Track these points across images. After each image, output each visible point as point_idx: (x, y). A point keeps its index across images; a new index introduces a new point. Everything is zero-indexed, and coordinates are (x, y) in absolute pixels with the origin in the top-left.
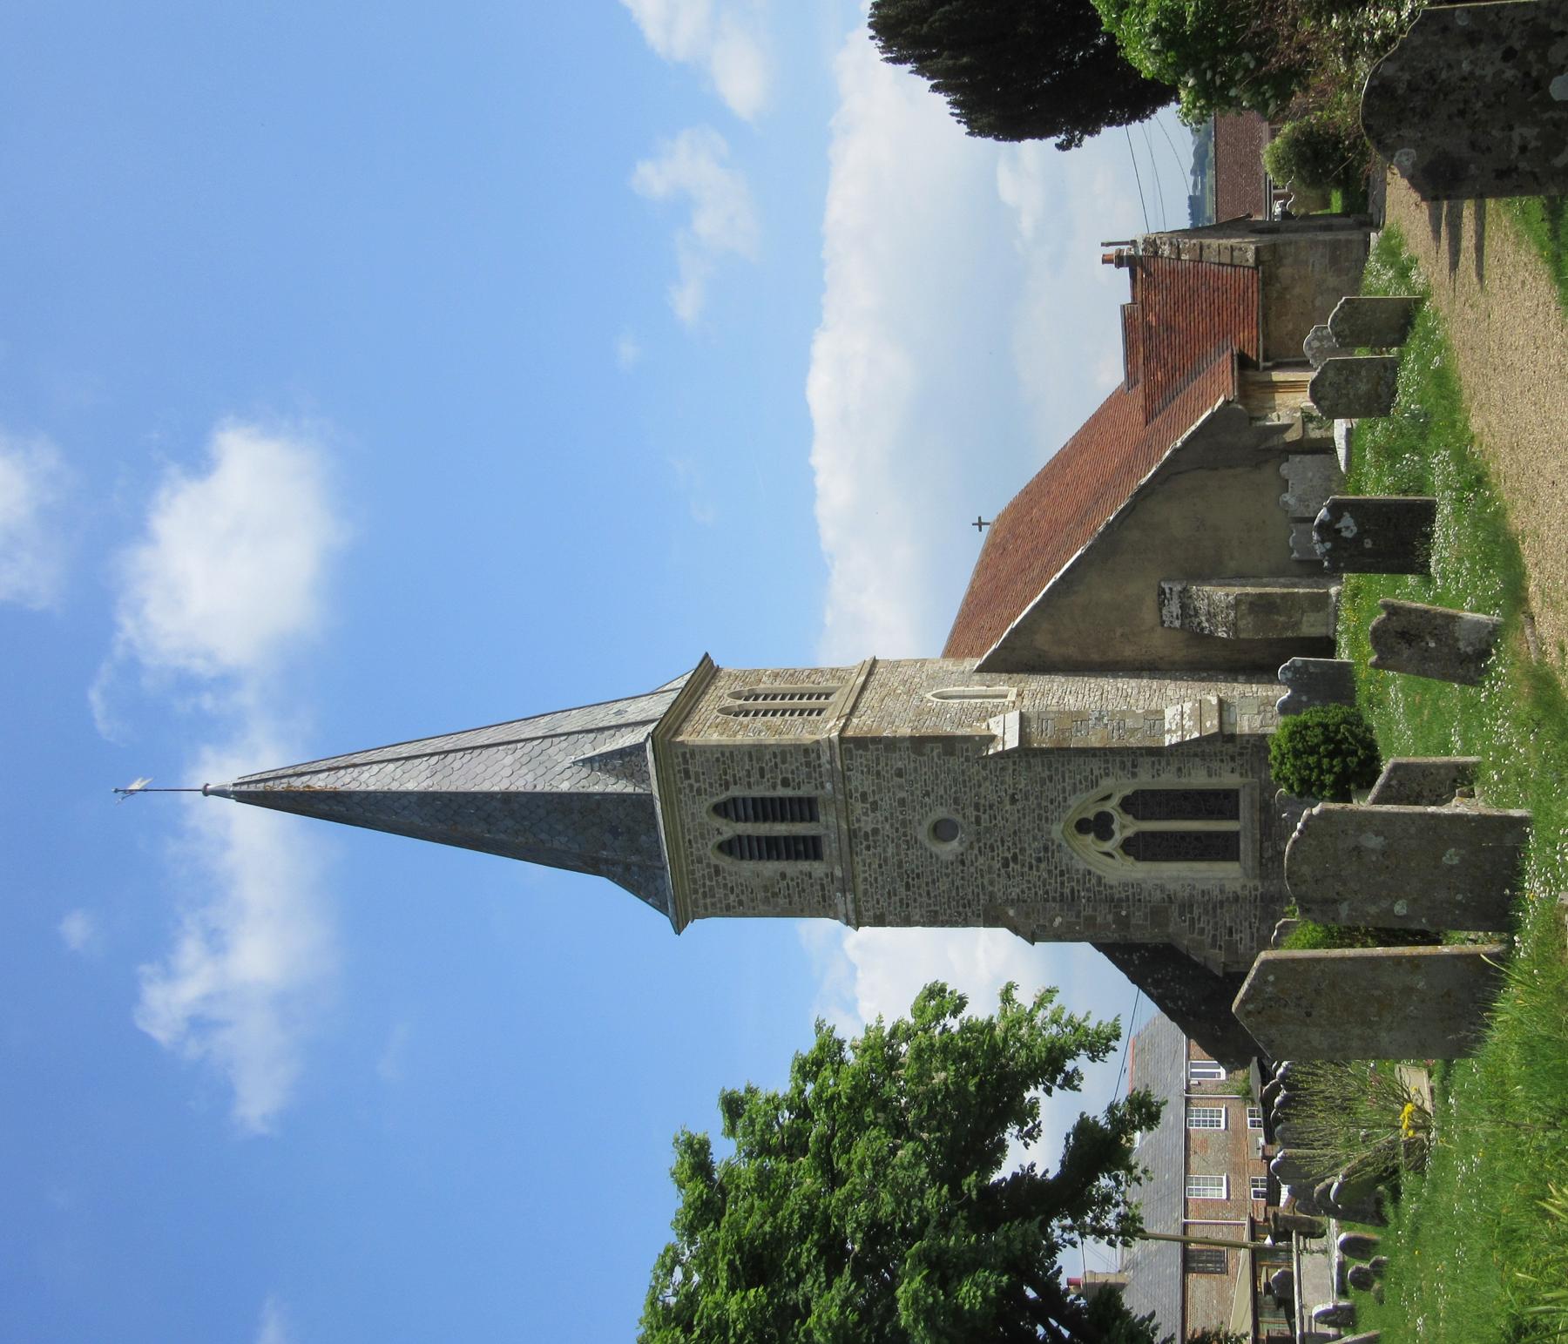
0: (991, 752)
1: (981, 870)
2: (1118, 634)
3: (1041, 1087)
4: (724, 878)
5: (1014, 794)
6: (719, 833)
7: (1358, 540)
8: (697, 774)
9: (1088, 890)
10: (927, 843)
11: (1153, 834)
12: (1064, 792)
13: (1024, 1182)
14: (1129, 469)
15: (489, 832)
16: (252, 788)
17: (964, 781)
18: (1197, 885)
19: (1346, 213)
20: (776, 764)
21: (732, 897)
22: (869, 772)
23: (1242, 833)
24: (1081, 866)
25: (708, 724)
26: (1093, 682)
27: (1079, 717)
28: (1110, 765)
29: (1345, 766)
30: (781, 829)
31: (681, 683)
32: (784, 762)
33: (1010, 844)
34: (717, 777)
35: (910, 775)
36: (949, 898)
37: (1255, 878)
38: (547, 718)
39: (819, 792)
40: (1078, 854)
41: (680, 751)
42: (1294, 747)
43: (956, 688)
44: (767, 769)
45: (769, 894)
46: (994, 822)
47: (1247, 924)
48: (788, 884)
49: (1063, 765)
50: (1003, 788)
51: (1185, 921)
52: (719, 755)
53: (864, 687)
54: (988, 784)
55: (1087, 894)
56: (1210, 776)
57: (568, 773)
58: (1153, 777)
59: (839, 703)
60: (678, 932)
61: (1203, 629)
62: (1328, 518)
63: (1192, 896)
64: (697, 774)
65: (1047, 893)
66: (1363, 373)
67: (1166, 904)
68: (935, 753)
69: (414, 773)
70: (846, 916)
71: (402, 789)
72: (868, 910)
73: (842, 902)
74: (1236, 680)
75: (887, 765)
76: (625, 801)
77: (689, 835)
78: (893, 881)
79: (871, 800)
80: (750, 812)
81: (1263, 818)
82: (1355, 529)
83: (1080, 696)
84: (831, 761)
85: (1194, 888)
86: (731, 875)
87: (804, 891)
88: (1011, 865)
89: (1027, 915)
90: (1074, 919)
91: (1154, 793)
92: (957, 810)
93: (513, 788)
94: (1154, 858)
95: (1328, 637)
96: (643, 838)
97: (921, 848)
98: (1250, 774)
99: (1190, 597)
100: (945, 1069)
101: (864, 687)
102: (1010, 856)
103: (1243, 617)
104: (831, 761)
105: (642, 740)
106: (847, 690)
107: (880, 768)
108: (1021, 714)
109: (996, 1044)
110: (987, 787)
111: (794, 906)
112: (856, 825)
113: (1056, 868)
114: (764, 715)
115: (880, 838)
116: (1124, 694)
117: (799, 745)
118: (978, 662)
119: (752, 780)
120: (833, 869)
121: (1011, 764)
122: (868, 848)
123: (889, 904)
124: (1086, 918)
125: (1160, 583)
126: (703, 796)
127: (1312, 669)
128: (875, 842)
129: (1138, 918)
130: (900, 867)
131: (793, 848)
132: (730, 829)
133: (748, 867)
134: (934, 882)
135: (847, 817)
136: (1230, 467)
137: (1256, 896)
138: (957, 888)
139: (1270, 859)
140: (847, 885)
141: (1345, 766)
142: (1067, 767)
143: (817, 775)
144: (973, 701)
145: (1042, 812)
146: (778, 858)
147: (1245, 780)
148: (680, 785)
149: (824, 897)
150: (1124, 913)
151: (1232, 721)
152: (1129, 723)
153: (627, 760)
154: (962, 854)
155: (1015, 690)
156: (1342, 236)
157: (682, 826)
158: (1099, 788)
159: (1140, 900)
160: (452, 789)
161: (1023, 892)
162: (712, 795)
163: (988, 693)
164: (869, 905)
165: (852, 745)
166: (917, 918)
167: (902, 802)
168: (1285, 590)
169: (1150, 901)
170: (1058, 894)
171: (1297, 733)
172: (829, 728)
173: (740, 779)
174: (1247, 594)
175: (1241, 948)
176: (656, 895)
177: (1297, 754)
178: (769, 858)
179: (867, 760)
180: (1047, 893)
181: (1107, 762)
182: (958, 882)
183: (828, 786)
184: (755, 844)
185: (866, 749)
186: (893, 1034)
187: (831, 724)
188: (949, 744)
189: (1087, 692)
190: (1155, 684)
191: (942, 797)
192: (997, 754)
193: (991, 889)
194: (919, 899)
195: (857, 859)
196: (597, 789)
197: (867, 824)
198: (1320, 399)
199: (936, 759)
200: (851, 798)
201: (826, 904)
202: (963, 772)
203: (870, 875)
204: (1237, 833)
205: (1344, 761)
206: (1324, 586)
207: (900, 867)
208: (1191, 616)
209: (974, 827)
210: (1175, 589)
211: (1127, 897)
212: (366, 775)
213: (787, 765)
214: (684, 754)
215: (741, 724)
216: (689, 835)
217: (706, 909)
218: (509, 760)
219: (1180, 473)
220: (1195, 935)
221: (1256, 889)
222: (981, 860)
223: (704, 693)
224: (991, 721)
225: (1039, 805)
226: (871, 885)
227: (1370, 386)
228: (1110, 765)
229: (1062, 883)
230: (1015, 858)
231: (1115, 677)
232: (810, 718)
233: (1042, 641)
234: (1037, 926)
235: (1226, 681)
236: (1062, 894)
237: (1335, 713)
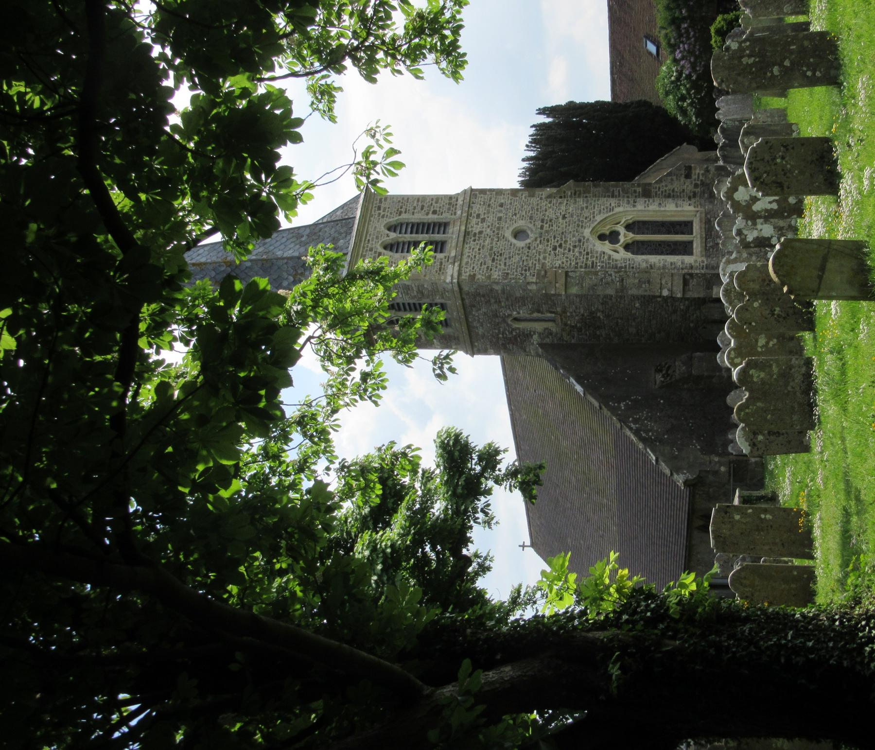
6: (388, 236)
9: (603, 262)
12: (594, 213)
17: (537, 209)
22: (484, 204)
37: (702, 256)
41: (379, 197)
54: (551, 210)
55: (601, 264)
56: (677, 207)
64: (385, 209)
65: (577, 263)
68: (524, 195)
72: (465, 273)
78: (485, 257)
79: (482, 217)
80: (409, 230)
81: (707, 226)
88: (558, 249)
112: (470, 229)
115: (483, 235)
122: (474, 240)
123: (480, 269)
134: (510, 258)
145: (580, 223)
148: (373, 213)
159: (633, 268)
161: (563, 263)
164: (468, 270)
167: (500, 219)
180: (577, 263)
182: (525, 258)
193: (543, 261)
194: (499, 267)
199: (523, 198)
211: (626, 266)
214: (381, 200)
221: (703, 262)
222: (540, 246)
225: (579, 220)
226: (472, 259)
229: (587, 259)
236: (586, 264)
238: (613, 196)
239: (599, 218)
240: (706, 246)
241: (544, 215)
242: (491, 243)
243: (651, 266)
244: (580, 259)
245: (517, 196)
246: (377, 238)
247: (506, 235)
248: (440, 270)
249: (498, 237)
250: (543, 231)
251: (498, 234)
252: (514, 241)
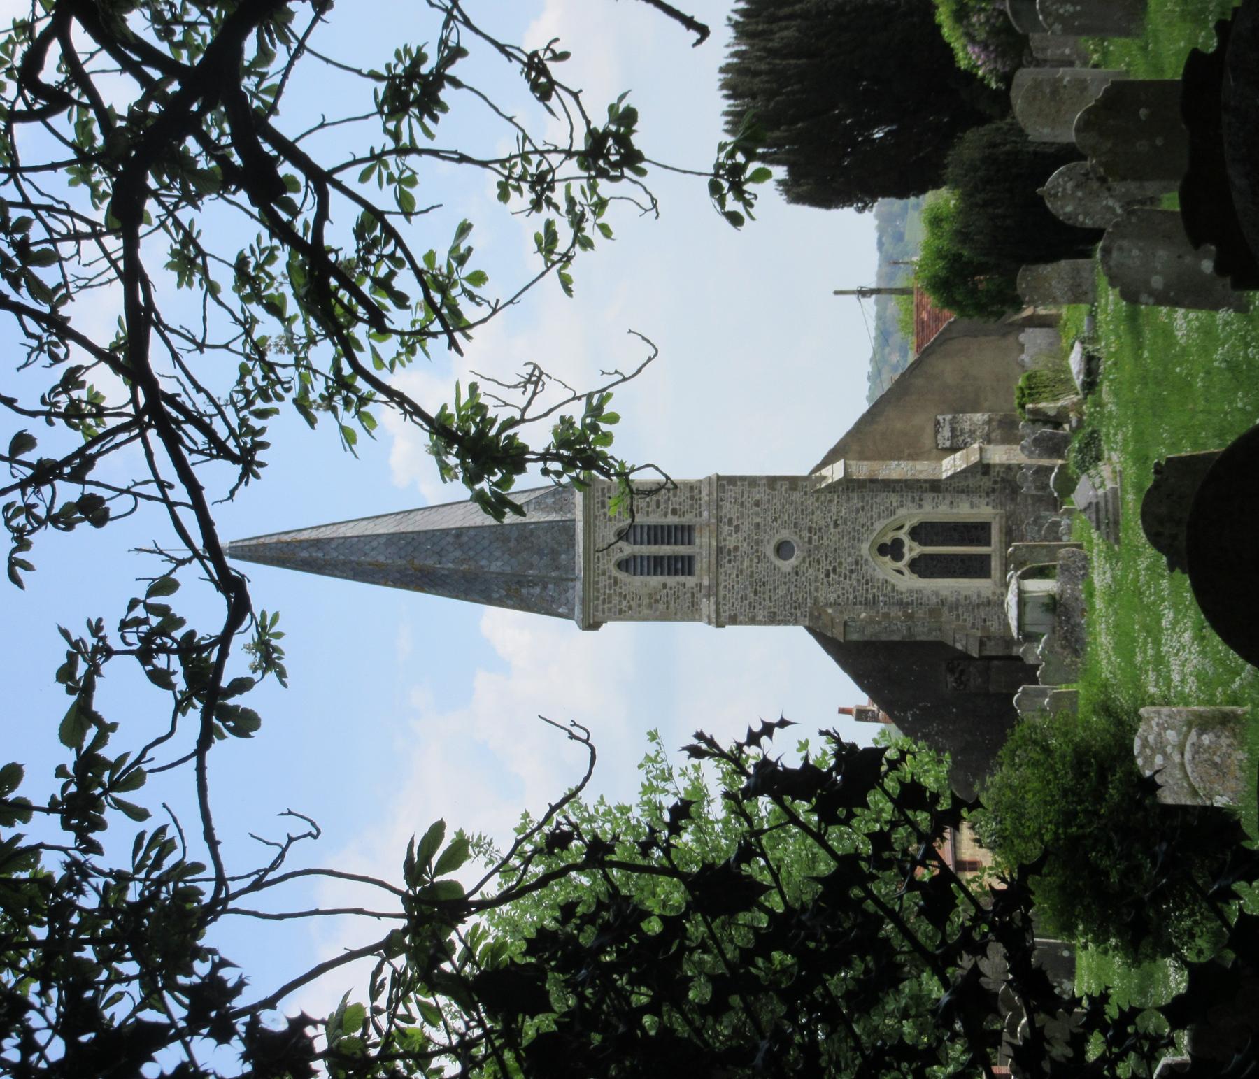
4: (621, 588)
6: (621, 551)
9: (885, 595)
15: (440, 563)
20: (669, 499)
21: (625, 603)
23: (993, 554)
44: (662, 501)
47: (996, 617)
56: (972, 507)
63: (958, 600)
68: (784, 488)
70: (709, 617)
72: (724, 612)
73: (707, 606)
78: (746, 588)
79: (735, 523)
80: (645, 537)
86: (625, 585)
87: (678, 598)
88: (832, 575)
94: (932, 575)
103: (993, 431)
112: (723, 544)
115: (739, 553)
119: (650, 510)
122: (730, 562)
124: (883, 614)
129: (920, 614)
130: (751, 576)
132: (628, 549)
133: (638, 580)
134: (775, 589)
136: (986, 335)
146: (662, 574)
149: (693, 602)
159: (921, 604)
164: (727, 608)
166: (760, 618)
167: (757, 526)
175: (992, 629)
176: (565, 605)
178: (655, 574)
180: (855, 598)
181: (902, 496)
182: (793, 589)
185: (735, 485)
195: (722, 570)
197: (730, 543)
204: (987, 557)
207: (751, 576)
209: (807, 545)
213: (677, 499)
214: (603, 489)
219: (951, 339)
220: (960, 622)
222: (810, 571)
225: (854, 528)
229: (867, 590)
230: (834, 570)
236: (866, 599)
238: (894, 492)
239: (878, 526)
241: (811, 520)
242: (751, 567)
243: (942, 600)
248: (693, 606)
249: (758, 557)
251: (757, 551)
252: (778, 562)
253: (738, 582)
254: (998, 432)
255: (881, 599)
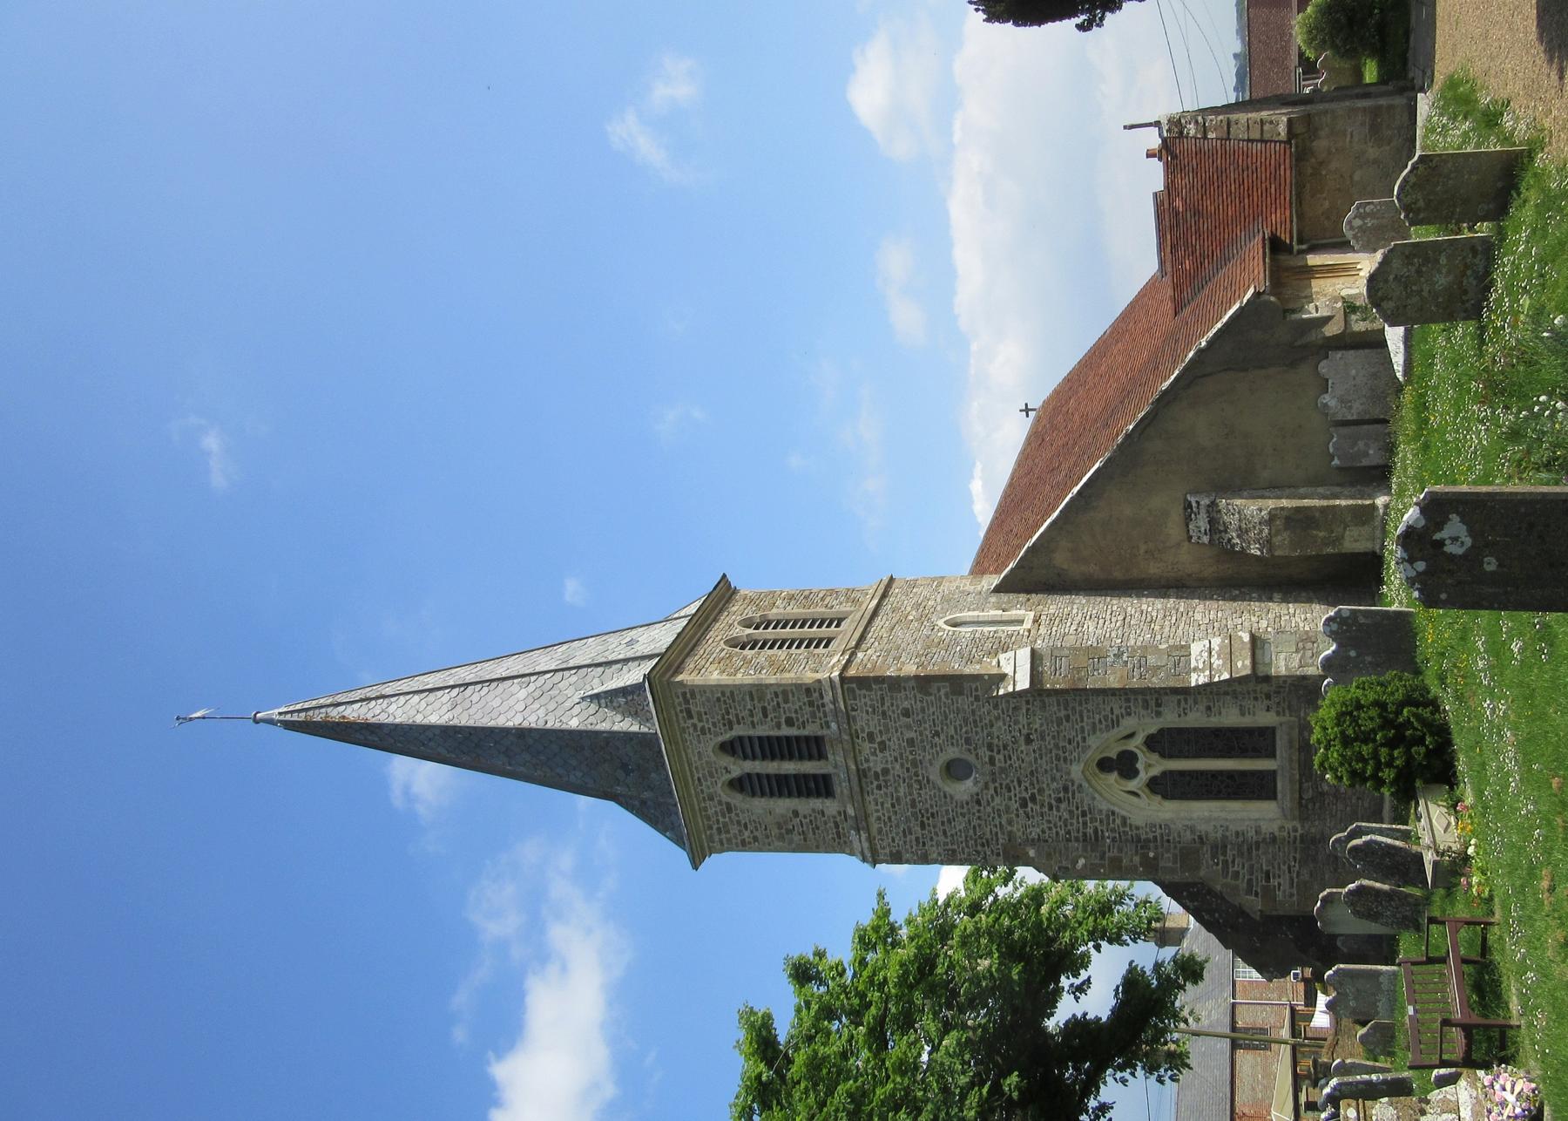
0: (1001, 692)
1: (998, 810)
2: (1142, 551)
3: (1091, 944)
4: (737, 815)
5: (1028, 735)
6: (728, 772)
7: (1472, 558)
8: (699, 714)
9: (1113, 830)
10: (939, 782)
11: (1182, 773)
12: (1083, 731)
13: (1078, 1026)
14: (1155, 368)
15: (510, 765)
16: (295, 718)
17: (975, 721)
18: (1231, 827)
19: (1383, 80)
20: (778, 704)
21: (747, 834)
23: (1279, 772)
24: (1104, 806)
25: (711, 660)
26: (1115, 603)
27: (1095, 654)
28: (1131, 704)
29: (1409, 759)
30: (789, 767)
31: (692, 609)
32: (786, 701)
33: (1027, 784)
34: (720, 717)
35: (918, 714)
36: (966, 837)
37: (1294, 819)
38: (565, 647)
39: (825, 732)
40: (1101, 795)
41: (680, 691)
42: (1343, 733)
43: (971, 613)
45: (783, 831)
46: (1009, 762)
47: (1285, 868)
48: (801, 822)
49: (1080, 704)
50: (1017, 728)
51: (1217, 864)
52: (719, 695)
53: (875, 613)
54: (1000, 723)
55: (1112, 835)
56: (1243, 714)
57: (577, 709)
58: (1180, 716)
59: (847, 633)
60: (696, 867)
61: (1233, 546)
62: (1423, 522)
63: (1224, 837)
64: (699, 714)
65: (1069, 833)
66: (1443, 261)
67: (1198, 845)
68: (943, 692)
69: (437, 705)
70: (862, 853)
71: (426, 722)
72: (884, 848)
74: (1270, 599)
75: (892, 705)
76: (631, 739)
77: (698, 772)
79: (878, 740)
82: (1468, 541)
83: (1101, 621)
84: (834, 701)
85: (1227, 827)
86: (743, 812)
87: (818, 828)
88: (1030, 805)
89: (1049, 856)
90: (1097, 861)
91: (1180, 731)
92: (969, 750)
93: (525, 724)
95: (1374, 553)
96: (653, 775)
97: (934, 788)
98: (1287, 712)
99: (1220, 511)
100: (990, 954)
101: (875, 613)
102: (1027, 796)
103: (1278, 532)
104: (834, 701)
105: (641, 680)
106: (860, 614)
107: (885, 708)
108: (1033, 652)
109: (1042, 922)
110: (1000, 727)
111: (808, 842)
112: (865, 765)
113: (1077, 809)
114: (771, 647)
115: (891, 777)
116: (1149, 619)
117: (801, 685)
118: (995, 580)
119: (755, 720)
120: (846, 807)
121: (1024, 703)
123: (905, 842)
124: (1112, 860)
125: (1186, 495)
126: (708, 735)
127: (1362, 620)
128: (886, 781)
131: (804, 785)
132: (739, 767)
133: (759, 805)
135: (855, 757)
136: (1262, 367)
137: (1295, 837)
138: (974, 827)
139: (1312, 800)
140: (861, 823)
141: (1409, 759)
142: (1084, 706)
143: (821, 714)
144: (986, 629)
145: (1061, 753)
146: (790, 795)
147: (1283, 719)
148: (683, 725)
149: (838, 834)
150: (1151, 855)
151: (1267, 660)
152: (1152, 660)
153: (630, 698)
154: (978, 795)
155: (1032, 614)
156: (1383, 102)
157: (690, 765)
158: (1121, 728)
159: (1168, 841)
160: (471, 723)
161: (1043, 832)
162: (716, 735)
163: (1004, 618)
165: (852, 685)
166: (935, 855)
167: (911, 742)
168: (1325, 503)
169: (1180, 842)
170: (1081, 834)
171: (1350, 712)
172: (826, 667)
173: (743, 718)
174: (1282, 509)
175: (1280, 895)
177: (1346, 741)
178: (781, 795)
179: (871, 700)
180: (1069, 833)
181: (1128, 700)
183: (834, 726)
184: (765, 782)
185: (870, 689)
186: (947, 904)
187: (835, 659)
188: (957, 683)
189: (1108, 617)
190: (1182, 605)
191: (952, 737)
192: (1007, 695)
193: (1009, 828)
196: (604, 727)
197: (876, 764)
198: (1382, 299)
200: (858, 738)
201: (842, 841)
202: (973, 712)
203: (884, 815)
204: (1274, 772)
205: (1408, 752)
206: (1371, 497)
208: (1220, 532)
209: (988, 767)
210: (1202, 503)
211: (1155, 837)
212: (394, 707)
214: (684, 694)
215: (744, 658)
216: (698, 772)
217: (722, 844)
218: (523, 694)
219: (1204, 376)
220: (1229, 880)
221: (1295, 830)
222: (997, 800)
223: (715, 620)
224: (1002, 657)
225: (1057, 746)
226: (885, 824)
227: (1451, 278)
228: (1131, 704)
229: (1085, 824)
230: (1033, 798)
231: (1138, 596)
232: (817, 651)
233: (1061, 559)
234: (1059, 868)
235: (1260, 600)
236: (1085, 834)
237: (1396, 685)
240: (1301, 798)
243: (1200, 837)
244: (1072, 824)
245: (931, 694)
246: (712, 776)
247: (931, 777)
249: (919, 782)
250: (996, 769)
253: (896, 813)
254: (1286, 535)
255: (1107, 834)
